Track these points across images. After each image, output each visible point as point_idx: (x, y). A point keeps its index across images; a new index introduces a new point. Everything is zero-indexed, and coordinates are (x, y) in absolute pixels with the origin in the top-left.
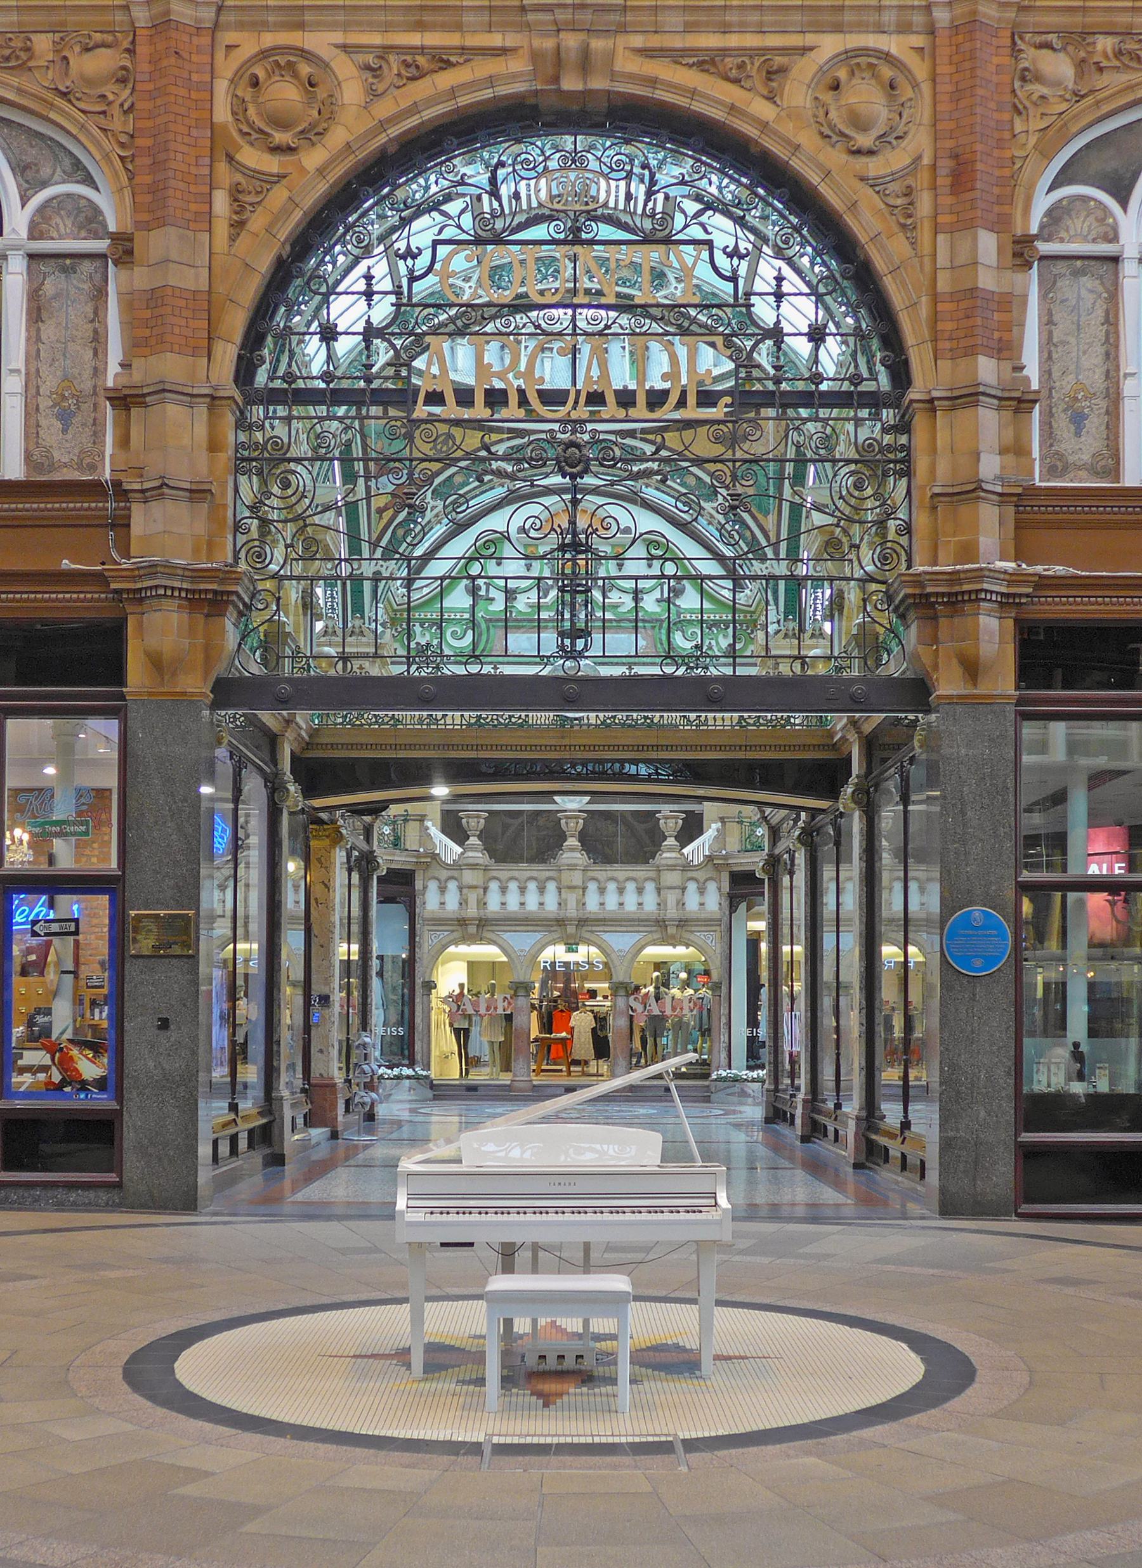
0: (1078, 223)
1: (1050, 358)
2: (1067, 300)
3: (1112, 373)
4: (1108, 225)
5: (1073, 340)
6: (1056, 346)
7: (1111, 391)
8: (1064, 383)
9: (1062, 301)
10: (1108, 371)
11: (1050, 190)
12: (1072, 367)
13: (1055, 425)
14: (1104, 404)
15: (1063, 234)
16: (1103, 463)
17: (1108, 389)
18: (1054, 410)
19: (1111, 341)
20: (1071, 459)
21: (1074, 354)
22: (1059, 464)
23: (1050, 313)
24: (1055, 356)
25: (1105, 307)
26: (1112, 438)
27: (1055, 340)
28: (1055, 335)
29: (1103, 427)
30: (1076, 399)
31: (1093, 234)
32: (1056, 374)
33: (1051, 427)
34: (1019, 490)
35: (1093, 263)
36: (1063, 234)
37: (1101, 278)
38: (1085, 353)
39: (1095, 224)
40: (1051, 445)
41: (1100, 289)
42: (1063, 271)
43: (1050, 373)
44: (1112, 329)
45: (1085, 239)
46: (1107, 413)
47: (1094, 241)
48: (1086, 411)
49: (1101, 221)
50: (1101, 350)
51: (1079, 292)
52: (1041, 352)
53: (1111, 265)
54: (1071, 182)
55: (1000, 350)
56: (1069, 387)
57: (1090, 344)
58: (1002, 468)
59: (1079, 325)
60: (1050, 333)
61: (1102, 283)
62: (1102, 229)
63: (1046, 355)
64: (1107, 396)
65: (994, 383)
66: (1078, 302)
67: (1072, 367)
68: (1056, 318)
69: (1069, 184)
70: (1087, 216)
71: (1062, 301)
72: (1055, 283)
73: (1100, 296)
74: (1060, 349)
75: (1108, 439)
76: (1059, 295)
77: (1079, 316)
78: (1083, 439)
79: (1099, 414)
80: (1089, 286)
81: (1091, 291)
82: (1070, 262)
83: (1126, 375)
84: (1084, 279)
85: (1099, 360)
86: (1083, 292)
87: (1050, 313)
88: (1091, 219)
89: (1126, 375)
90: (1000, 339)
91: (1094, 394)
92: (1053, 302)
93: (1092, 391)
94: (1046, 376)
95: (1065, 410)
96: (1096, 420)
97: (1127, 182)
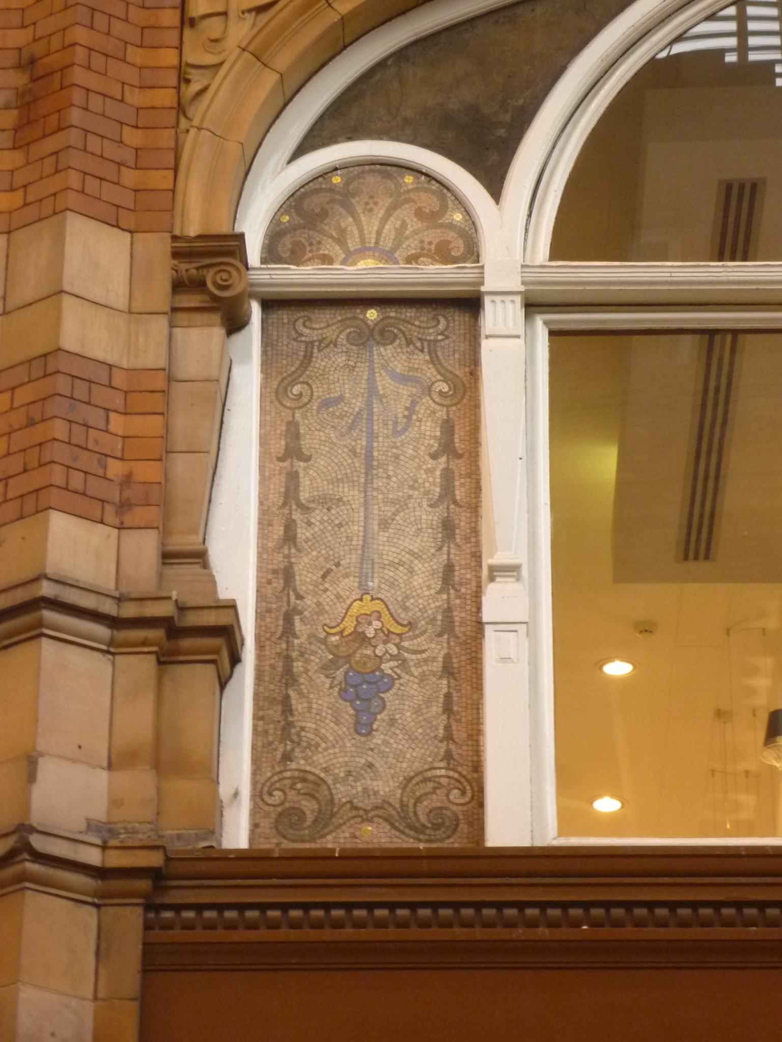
0: (371, 225)
1: (290, 537)
2: (341, 398)
3: (459, 574)
4: (451, 226)
5: (354, 496)
6: (305, 509)
7: (457, 616)
8: (325, 599)
9: (326, 404)
10: (449, 568)
11: (300, 151)
12: (350, 560)
13: (298, 705)
14: (437, 650)
15: (330, 248)
16: (436, 800)
17: (448, 611)
18: (298, 666)
19: (459, 494)
20: (341, 792)
21: (357, 528)
22: (309, 807)
23: (293, 433)
24: (302, 533)
25: (441, 414)
26: (459, 733)
27: (304, 496)
28: (305, 482)
29: (436, 708)
30: (361, 638)
31: (411, 246)
32: (305, 577)
33: (287, 709)
34: (154, 859)
35: (409, 313)
36: (330, 248)
37: (432, 349)
38: (384, 524)
39: (414, 224)
40: (287, 757)
41: (431, 372)
42: (330, 333)
43: (288, 575)
44: (460, 467)
45: (388, 256)
46: (448, 671)
47: (411, 259)
48: (386, 667)
49: (432, 218)
50: (430, 517)
51: (371, 380)
52: (264, 523)
53: (459, 319)
54: (353, 134)
55: (124, 506)
56: (340, 608)
57: (402, 504)
58: (115, 803)
59: (369, 457)
60: (293, 477)
61: (434, 361)
62: (432, 236)
63: (279, 531)
64: (448, 627)
65: (110, 585)
66: (369, 405)
67: (350, 560)
68: (306, 444)
69: (350, 139)
70: (394, 207)
71: (326, 404)
72: (308, 358)
73: (429, 390)
74: (317, 517)
75: (449, 737)
76: (319, 391)
77: (372, 436)
78: (378, 739)
79: (423, 678)
80: (399, 366)
81: (404, 379)
82: (349, 313)
83: (496, 572)
84: (387, 351)
85: (425, 541)
86: (384, 382)
87: (293, 433)
88: (405, 213)
89: (496, 572)
90: (127, 480)
91: (411, 625)
92: (301, 403)
93: (404, 617)
94: (279, 584)
95: (327, 668)
96: (414, 689)
97: (501, 132)
